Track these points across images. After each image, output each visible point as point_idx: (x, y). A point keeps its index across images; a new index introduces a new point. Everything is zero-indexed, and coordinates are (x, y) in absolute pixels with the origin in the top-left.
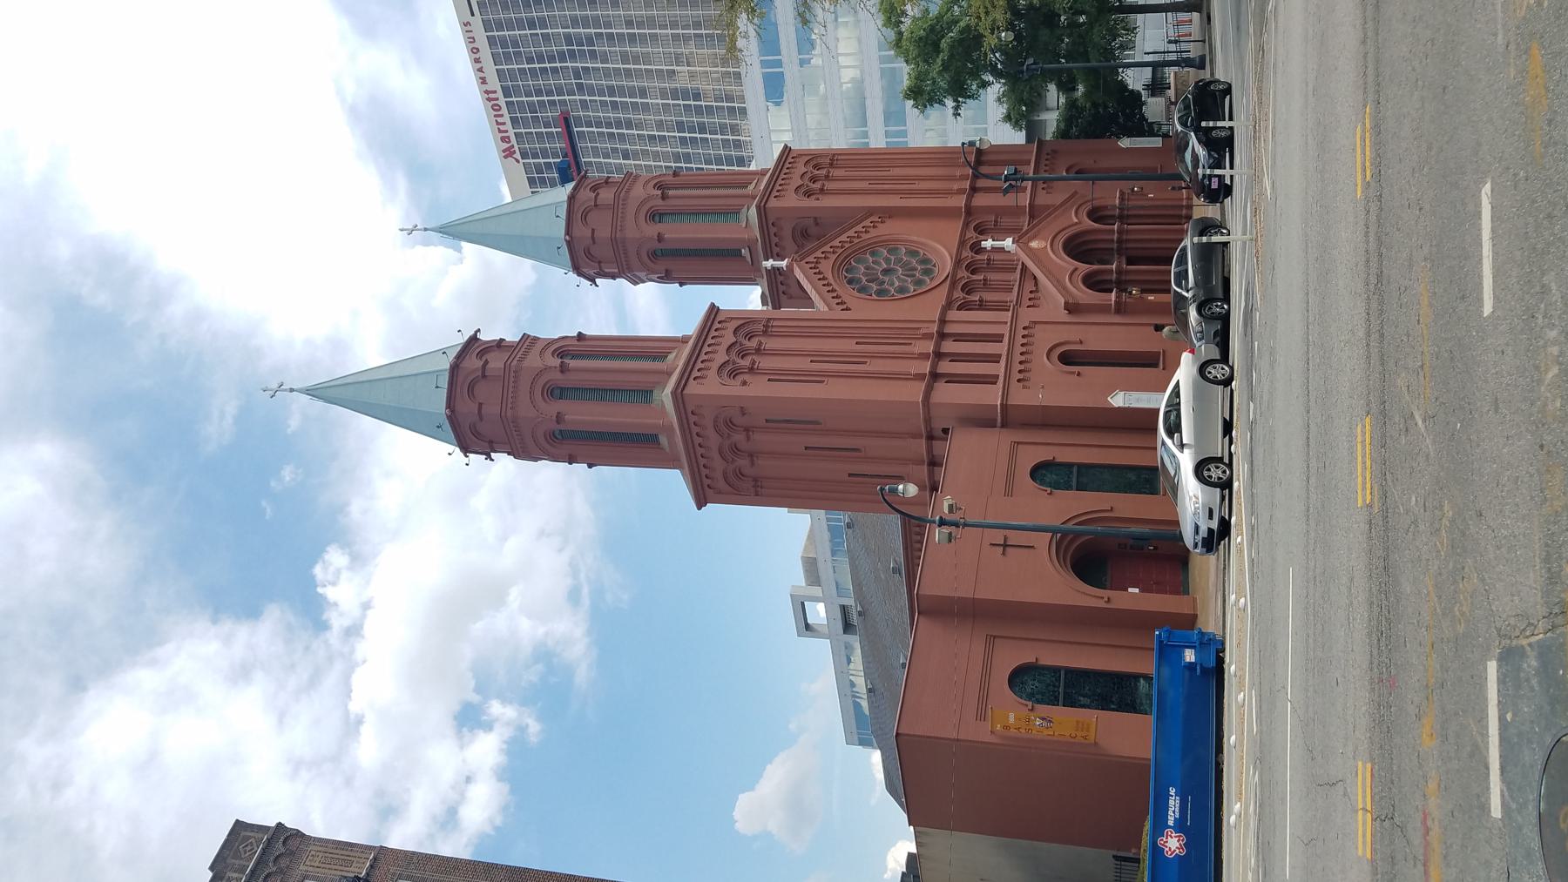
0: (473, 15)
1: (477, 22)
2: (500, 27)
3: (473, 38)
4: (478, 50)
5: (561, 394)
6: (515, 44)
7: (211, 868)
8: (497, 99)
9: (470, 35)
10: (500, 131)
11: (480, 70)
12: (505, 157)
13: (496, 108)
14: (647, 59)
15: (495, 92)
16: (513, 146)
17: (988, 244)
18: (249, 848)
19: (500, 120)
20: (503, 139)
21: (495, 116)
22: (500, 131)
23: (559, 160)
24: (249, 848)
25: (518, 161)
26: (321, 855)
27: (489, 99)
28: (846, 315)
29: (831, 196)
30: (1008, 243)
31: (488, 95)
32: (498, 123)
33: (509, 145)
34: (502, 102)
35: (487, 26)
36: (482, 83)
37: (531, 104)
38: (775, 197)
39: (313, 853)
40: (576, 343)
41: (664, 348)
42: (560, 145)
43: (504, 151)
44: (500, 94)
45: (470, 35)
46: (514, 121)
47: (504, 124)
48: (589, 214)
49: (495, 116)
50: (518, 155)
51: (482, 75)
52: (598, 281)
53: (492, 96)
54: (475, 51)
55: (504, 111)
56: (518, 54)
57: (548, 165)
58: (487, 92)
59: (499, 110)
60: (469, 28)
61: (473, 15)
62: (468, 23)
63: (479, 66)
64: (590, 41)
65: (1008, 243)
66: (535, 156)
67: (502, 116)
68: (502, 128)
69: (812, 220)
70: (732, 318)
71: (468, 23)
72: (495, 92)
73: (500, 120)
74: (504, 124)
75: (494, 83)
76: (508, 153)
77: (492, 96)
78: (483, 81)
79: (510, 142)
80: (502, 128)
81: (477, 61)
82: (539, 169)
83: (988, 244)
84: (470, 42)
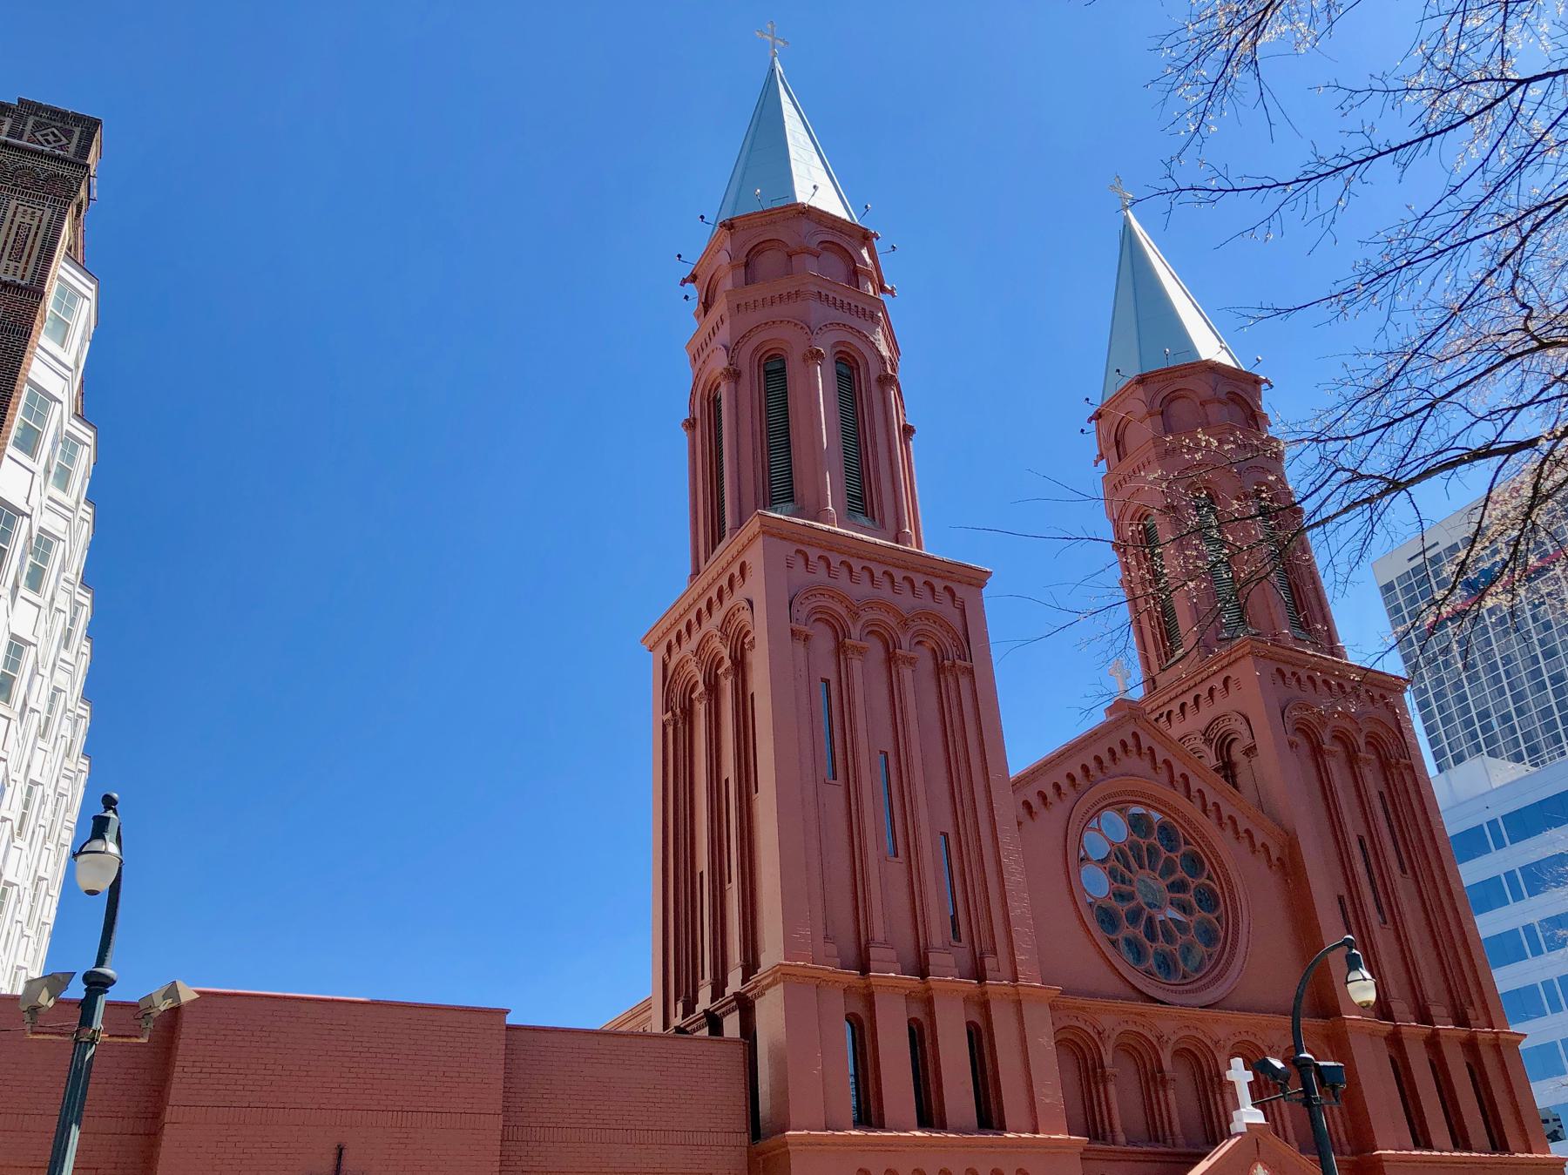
5: (776, 371)
7: (21, 101)
17: (1239, 1074)
18: (51, 138)
24: (51, 138)
26: (35, 223)
28: (1007, 809)
29: (1313, 772)
30: (1248, 1115)
38: (1278, 670)
39: (39, 213)
40: (874, 376)
41: (881, 507)
48: (1180, 400)
52: (1103, 464)
65: (1248, 1115)
69: (1248, 741)
70: (963, 611)
83: (1239, 1074)
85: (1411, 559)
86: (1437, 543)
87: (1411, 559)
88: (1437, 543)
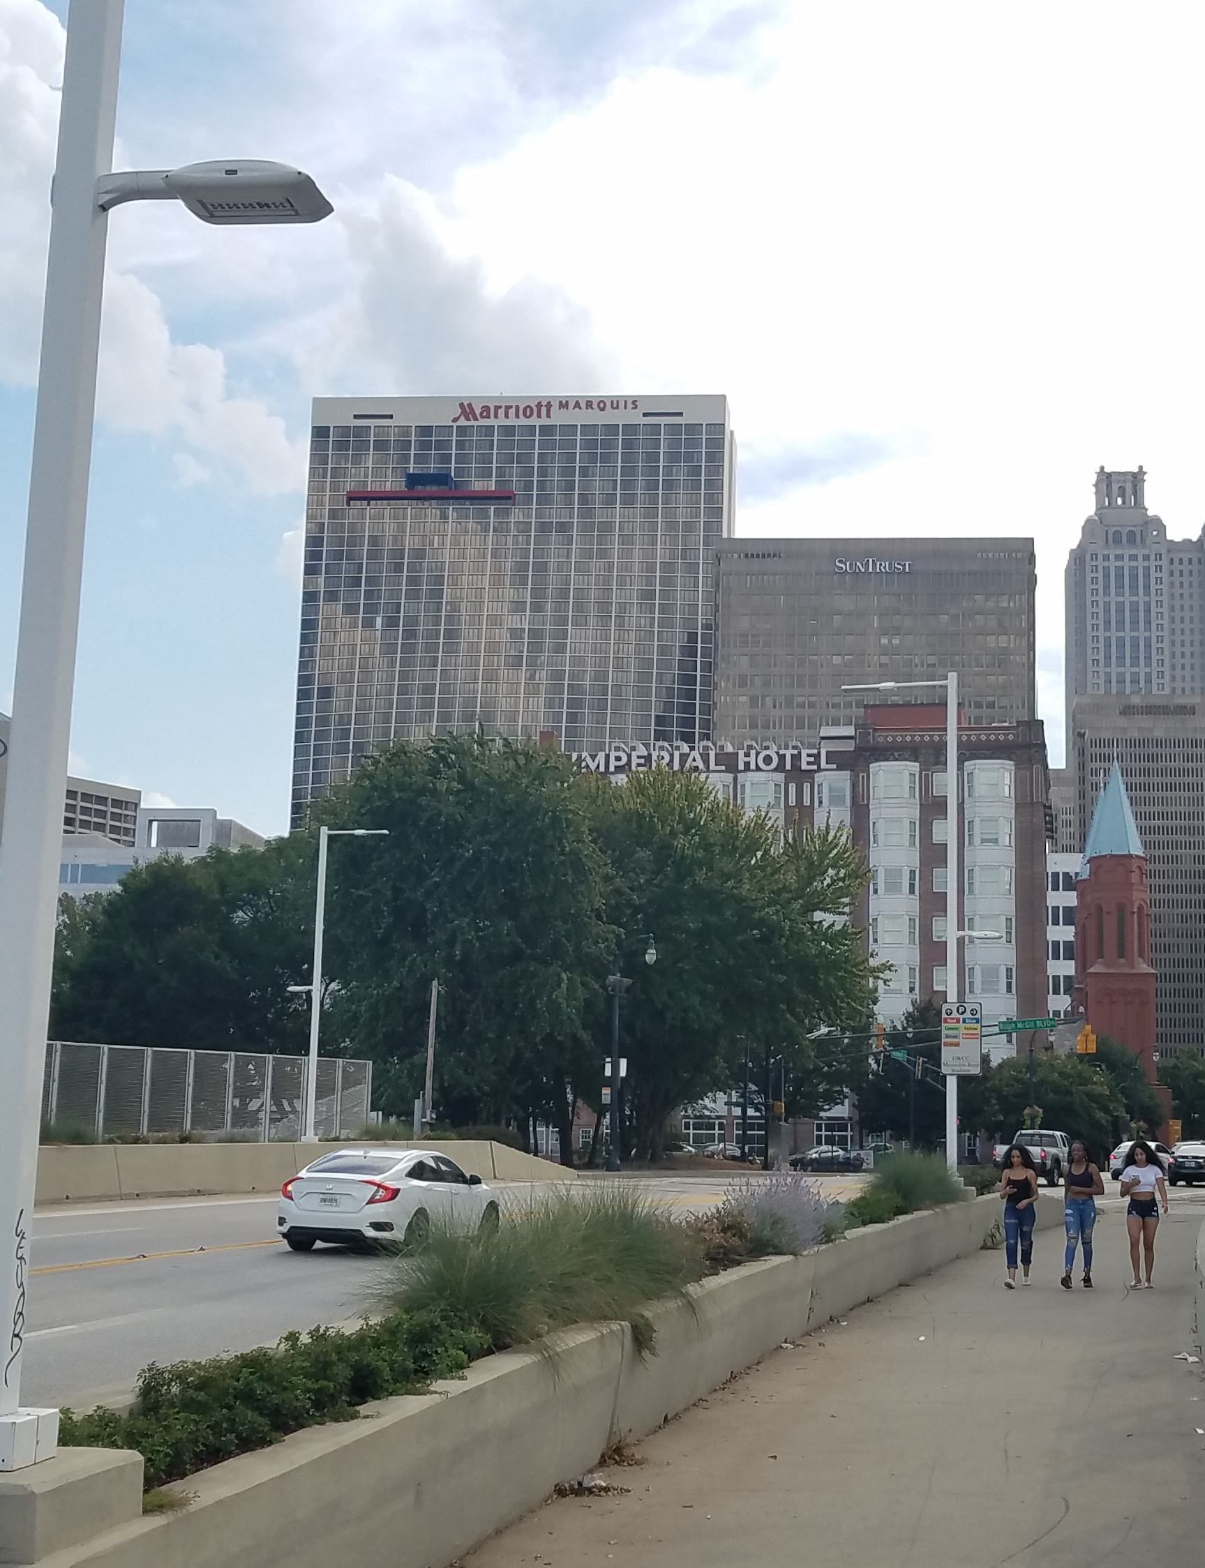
0: (645, 415)
1: (637, 419)
2: (628, 444)
3: (617, 408)
4: (603, 409)
6: (606, 458)
8: (539, 416)
9: (622, 405)
10: (497, 408)
11: (577, 405)
12: (462, 405)
13: (528, 411)
14: (580, 622)
15: (548, 416)
16: (476, 419)
19: (512, 412)
20: (486, 408)
21: (517, 407)
22: (497, 408)
23: (453, 474)
25: (455, 420)
27: (539, 405)
31: (543, 406)
32: (508, 408)
33: (478, 412)
34: (534, 421)
35: (630, 429)
36: (561, 402)
37: (529, 458)
42: (478, 486)
43: (470, 405)
44: (545, 421)
45: (622, 405)
46: (509, 430)
47: (507, 416)
49: (517, 407)
50: (463, 422)
51: (571, 405)
53: (544, 410)
54: (602, 405)
55: (523, 421)
56: (593, 458)
57: (446, 459)
58: (549, 405)
59: (525, 415)
60: (630, 405)
61: (645, 415)
62: (636, 407)
63: (583, 405)
64: (603, 554)
66: (460, 445)
67: (517, 416)
68: (501, 412)
71: (636, 407)
72: (548, 416)
73: (512, 412)
74: (507, 416)
75: (559, 418)
76: (467, 410)
77: (544, 410)
78: (564, 405)
79: (482, 417)
80: (501, 412)
81: (589, 404)
82: (441, 445)
84: (612, 402)
85: (356, 417)
86: (391, 417)
87: (356, 417)
88: (391, 417)
